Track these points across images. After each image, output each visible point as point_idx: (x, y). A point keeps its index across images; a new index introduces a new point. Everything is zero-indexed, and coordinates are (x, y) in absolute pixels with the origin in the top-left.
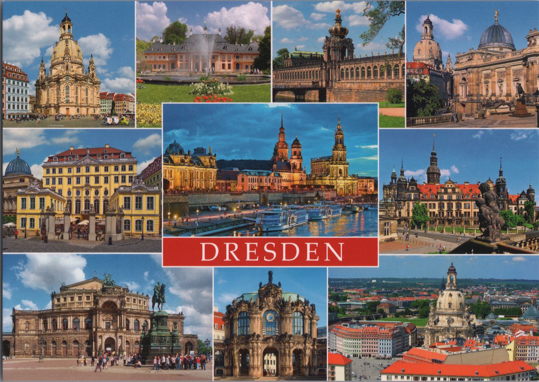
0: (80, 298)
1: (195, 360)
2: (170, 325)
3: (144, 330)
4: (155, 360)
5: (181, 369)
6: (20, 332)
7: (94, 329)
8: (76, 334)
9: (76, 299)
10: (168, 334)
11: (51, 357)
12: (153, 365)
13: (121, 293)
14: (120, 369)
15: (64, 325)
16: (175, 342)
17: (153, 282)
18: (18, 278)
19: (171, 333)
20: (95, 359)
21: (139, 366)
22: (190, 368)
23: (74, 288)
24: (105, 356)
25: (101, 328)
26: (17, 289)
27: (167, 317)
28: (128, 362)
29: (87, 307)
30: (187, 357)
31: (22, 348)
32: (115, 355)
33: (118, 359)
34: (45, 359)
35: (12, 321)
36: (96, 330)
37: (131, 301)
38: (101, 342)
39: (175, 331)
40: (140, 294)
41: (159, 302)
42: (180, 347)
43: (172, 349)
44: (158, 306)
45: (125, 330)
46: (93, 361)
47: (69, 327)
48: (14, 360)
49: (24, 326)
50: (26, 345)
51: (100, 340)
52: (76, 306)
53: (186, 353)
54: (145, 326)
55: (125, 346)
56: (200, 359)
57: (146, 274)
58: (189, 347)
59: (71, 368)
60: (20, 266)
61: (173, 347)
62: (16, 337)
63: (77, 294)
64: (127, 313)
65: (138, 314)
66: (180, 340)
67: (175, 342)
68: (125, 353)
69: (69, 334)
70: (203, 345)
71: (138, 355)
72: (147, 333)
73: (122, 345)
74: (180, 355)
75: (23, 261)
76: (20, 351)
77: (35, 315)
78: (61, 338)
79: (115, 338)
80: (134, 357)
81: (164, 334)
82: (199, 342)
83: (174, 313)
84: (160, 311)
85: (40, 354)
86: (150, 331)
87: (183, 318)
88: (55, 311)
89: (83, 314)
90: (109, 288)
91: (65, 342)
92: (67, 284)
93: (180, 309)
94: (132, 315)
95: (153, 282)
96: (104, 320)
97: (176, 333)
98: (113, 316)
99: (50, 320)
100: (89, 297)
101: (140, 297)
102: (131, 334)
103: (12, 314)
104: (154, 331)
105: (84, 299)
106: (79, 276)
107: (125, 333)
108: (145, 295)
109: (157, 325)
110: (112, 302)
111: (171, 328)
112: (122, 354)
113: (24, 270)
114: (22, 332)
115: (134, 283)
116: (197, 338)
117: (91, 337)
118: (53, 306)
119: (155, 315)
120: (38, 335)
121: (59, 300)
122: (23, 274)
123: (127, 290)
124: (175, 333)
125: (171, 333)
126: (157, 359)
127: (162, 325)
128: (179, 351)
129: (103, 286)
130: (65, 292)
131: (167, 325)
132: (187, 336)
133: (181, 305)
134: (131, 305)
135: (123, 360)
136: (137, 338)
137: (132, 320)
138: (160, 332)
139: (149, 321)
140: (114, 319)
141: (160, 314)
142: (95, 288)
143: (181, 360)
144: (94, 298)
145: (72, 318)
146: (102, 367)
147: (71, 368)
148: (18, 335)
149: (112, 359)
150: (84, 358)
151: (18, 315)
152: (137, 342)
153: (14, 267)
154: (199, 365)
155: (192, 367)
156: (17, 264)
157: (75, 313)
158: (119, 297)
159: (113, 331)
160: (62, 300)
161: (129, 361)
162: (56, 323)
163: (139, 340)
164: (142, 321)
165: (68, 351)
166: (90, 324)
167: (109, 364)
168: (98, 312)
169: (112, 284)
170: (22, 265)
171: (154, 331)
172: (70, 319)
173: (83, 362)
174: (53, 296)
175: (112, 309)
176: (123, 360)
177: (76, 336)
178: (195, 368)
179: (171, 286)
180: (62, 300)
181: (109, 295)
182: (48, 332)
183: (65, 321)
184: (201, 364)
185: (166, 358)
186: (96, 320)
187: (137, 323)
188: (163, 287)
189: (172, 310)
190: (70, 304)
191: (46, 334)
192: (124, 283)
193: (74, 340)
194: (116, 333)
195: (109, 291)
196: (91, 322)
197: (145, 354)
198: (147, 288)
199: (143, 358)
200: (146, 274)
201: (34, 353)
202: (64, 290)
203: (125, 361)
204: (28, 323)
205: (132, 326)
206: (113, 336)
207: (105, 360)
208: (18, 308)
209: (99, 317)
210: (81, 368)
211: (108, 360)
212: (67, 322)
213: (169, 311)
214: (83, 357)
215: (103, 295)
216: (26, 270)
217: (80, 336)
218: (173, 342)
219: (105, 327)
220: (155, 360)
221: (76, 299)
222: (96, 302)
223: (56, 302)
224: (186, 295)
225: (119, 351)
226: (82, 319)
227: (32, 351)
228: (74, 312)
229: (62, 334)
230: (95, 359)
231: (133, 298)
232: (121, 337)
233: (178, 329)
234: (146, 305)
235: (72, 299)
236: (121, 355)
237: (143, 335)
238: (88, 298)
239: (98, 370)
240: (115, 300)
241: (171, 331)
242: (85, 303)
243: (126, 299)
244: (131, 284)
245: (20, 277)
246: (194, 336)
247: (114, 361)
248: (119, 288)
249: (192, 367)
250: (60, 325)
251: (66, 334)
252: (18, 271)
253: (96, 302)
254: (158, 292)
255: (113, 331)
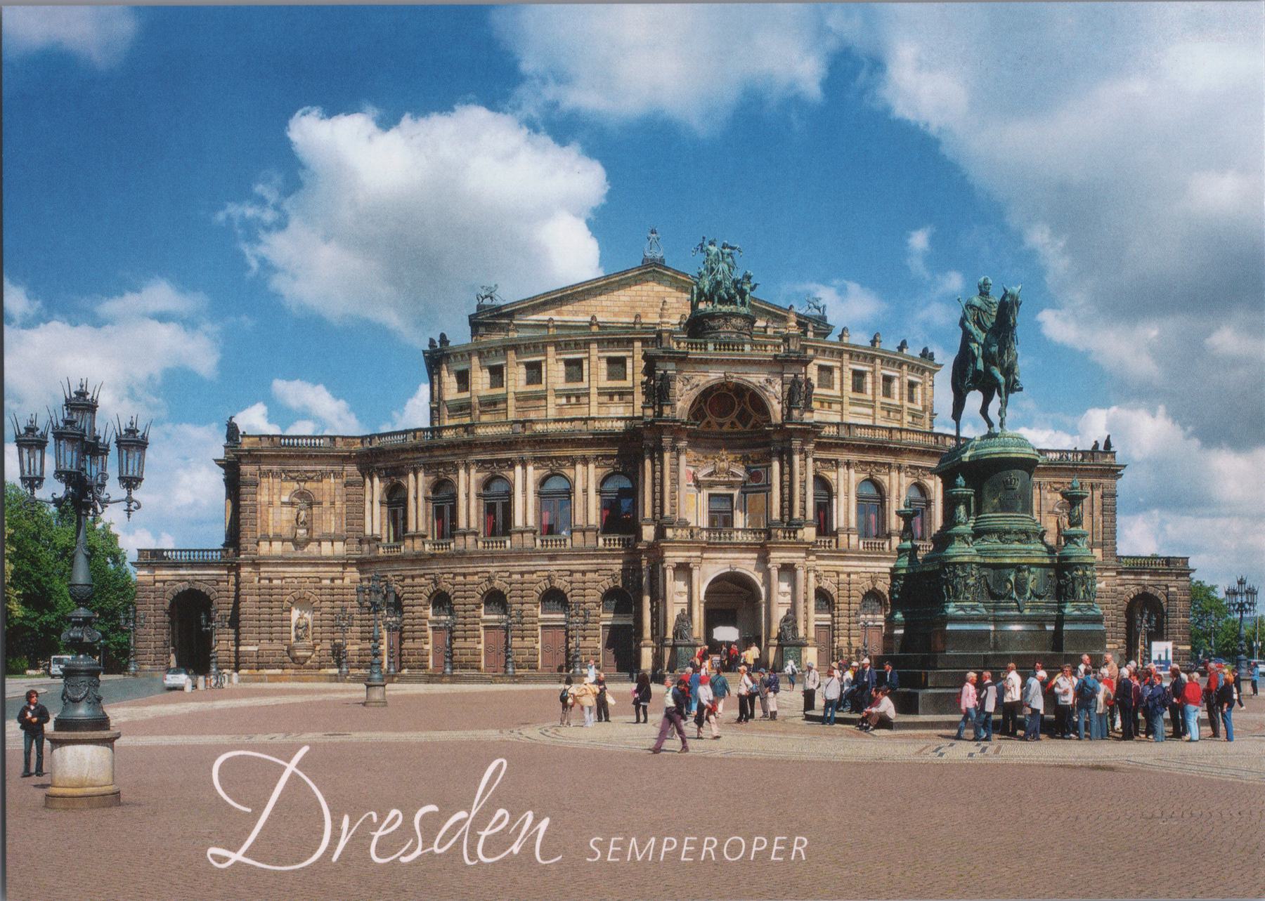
0: (574, 368)
1: (1178, 687)
2: (1046, 503)
3: (907, 533)
4: (969, 689)
5: (1106, 734)
6: (264, 548)
7: (648, 532)
8: (552, 558)
9: (555, 373)
10: (1036, 552)
11: (430, 679)
12: (957, 718)
13: (786, 339)
14: (786, 739)
15: (490, 510)
16: (1073, 596)
17: (955, 282)
18: (254, 264)
19: (1051, 550)
20: (655, 688)
21: (884, 723)
22: (1151, 730)
23: (543, 317)
24: (706, 668)
25: (684, 525)
26: (248, 322)
27: (1028, 465)
28: (829, 703)
29: (613, 416)
30: (1135, 673)
31: (274, 625)
32: (760, 664)
33: (773, 686)
34: (394, 689)
35: (223, 490)
36: (660, 533)
37: (842, 384)
38: (683, 598)
39: (1070, 538)
40: (890, 345)
41: (989, 388)
42: (1098, 620)
43: (1058, 634)
44: (984, 411)
45: (809, 533)
46: (644, 695)
47: (518, 522)
48: (233, 694)
49: (287, 514)
50: (295, 614)
51: (681, 586)
52: (552, 413)
53: (1130, 654)
54: (914, 515)
55: (811, 620)
56: (1203, 685)
57: (919, 240)
58: (1143, 626)
59: (532, 733)
60: (262, 201)
61: (1060, 621)
62: (245, 572)
63: (557, 345)
64: (820, 446)
65: (878, 450)
66: (1101, 585)
67: (1073, 596)
68: (811, 655)
69: (521, 554)
70: (1219, 608)
71: (878, 662)
72: (925, 548)
73: (793, 611)
74: (1097, 663)
75: (278, 179)
76: (265, 645)
77: (345, 459)
78: (476, 578)
79: (758, 578)
80: (859, 674)
81: (1013, 552)
82: (1199, 594)
83: (1065, 442)
84: (990, 436)
85: (370, 661)
86: (943, 540)
87: (1113, 472)
88: (448, 434)
89: (590, 452)
90: (727, 316)
91: (495, 599)
92: (507, 295)
93: (1095, 426)
94: (844, 456)
95: (955, 282)
96: (699, 485)
97: (1079, 550)
98: (745, 459)
99: (417, 485)
100: (621, 361)
101: (889, 361)
102: (841, 555)
103: (221, 455)
104: (962, 537)
105: (597, 374)
106: (572, 254)
107: (809, 548)
108: (913, 351)
109: (979, 510)
110: (741, 391)
111: (1050, 524)
112: (798, 661)
113: (281, 225)
114: (277, 547)
115: (854, 287)
116: (1185, 572)
117: (632, 569)
118: (435, 412)
119: (966, 457)
120: (361, 564)
121: (463, 379)
122: (279, 247)
123: (821, 325)
124: (1072, 550)
125: (1051, 550)
126: (980, 686)
127: (1005, 507)
128: (1098, 640)
129: (694, 307)
130: (497, 337)
131: (1028, 508)
132: (1137, 566)
133: (1105, 404)
134: (840, 406)
135: (799, 689)
136: (874, 579)
137: (847, 482)
138: (991, 543)
139: (935, 486)
140: (754, 476)
141: (994, 450)
142: (652, 318)
143: (1103, 692)
144: (649, 371)
145: (533, 474)
146: (689, 726)
147: (532, 733)
148: (255, 564)
149: (742, 684)
150: (599, 682)
151: (254, 457)
152: (872, 595)
153: (233, 209)
154: (1196, 714)
155: (1163, 727)
156: (244, 194)
157: (549, 448)
158: (780, 363)
159: (750, 538)
160: (481, 382)
161: (834, 693)
162: (454, 497)
163: (884, 586)
164: (898, 487)
165: (516, 643)
166: (625, 504)
167: (727, 709)
168: (667, 440)
169: (739, 292)
170: (272, 197)
171: (962, 537)
172: (524, 482)
173: (590, 701)
174: (437, 358)
175: (743, 428)
176: (799, 689)
177: (553, 567)
178: (1179, 730)
179: (1054, 305)
180: (481, 382)
181: (726, 355)
182: (408, 547)
183: (497, 487)
184: (1211, 710)
185: (1025, 677)
186: (658, 484)
187: (873, 500)
188: (1007, 307)
189: (1058, 427)
190: (523, 398)
191: (401, 559)
192: (799, 288)
193: (544, 585)
194: (763, 552)
195: (726, 331)
196: (633, 493)
197: (915, 657)
198: (922, 315)
199: (905, 680)
200: (919, 240)
201: (338, 655)
202: (491, 327)
203: (809, 696)
204: (309, 500)
205: (845, 512)
206: (746, 565)
207: (705, 693)
208: (254, 420)
209: (676, 470)
210: (581, 733)
211: (720, 690)
212: (509, 494)
213: (1036, 432)
214: (592, 674)
215: (695, 354)
216: (295, 223)
217: (577, 564)
218: (1063, 592)
219: (704, 522)
220: (969, 689)
221: (555, 373)
222: (658, 392)
223: (451, 389)
224: (1130, 347)
225: (780, 647)
226: (587, 479)
227: (327, 645)
228: (542, 441)
229: (484, 557)
230: (655, 688)
231: (850, 366)
232: (788, 570)
233: (1085, 527)
234: (918, 406)
235: (534, 372)
236: (790, 666)
237: (904, 562)
238: (617, 367)
239: (673, 743)
240: (756, 378)
241: (1051, 539)
242: (602, 392)
243: (813, 372)
244: (842, 292)
245: (263, 262)
246: (1174, 566)
247: (752, 696)
248: (778, 316)
249: (1163, 727)
250: (470, 512)
251: (504, 557)
252: (252, 231)
253: (658, 392)
254: (981, 337)
255: (750, 538)
